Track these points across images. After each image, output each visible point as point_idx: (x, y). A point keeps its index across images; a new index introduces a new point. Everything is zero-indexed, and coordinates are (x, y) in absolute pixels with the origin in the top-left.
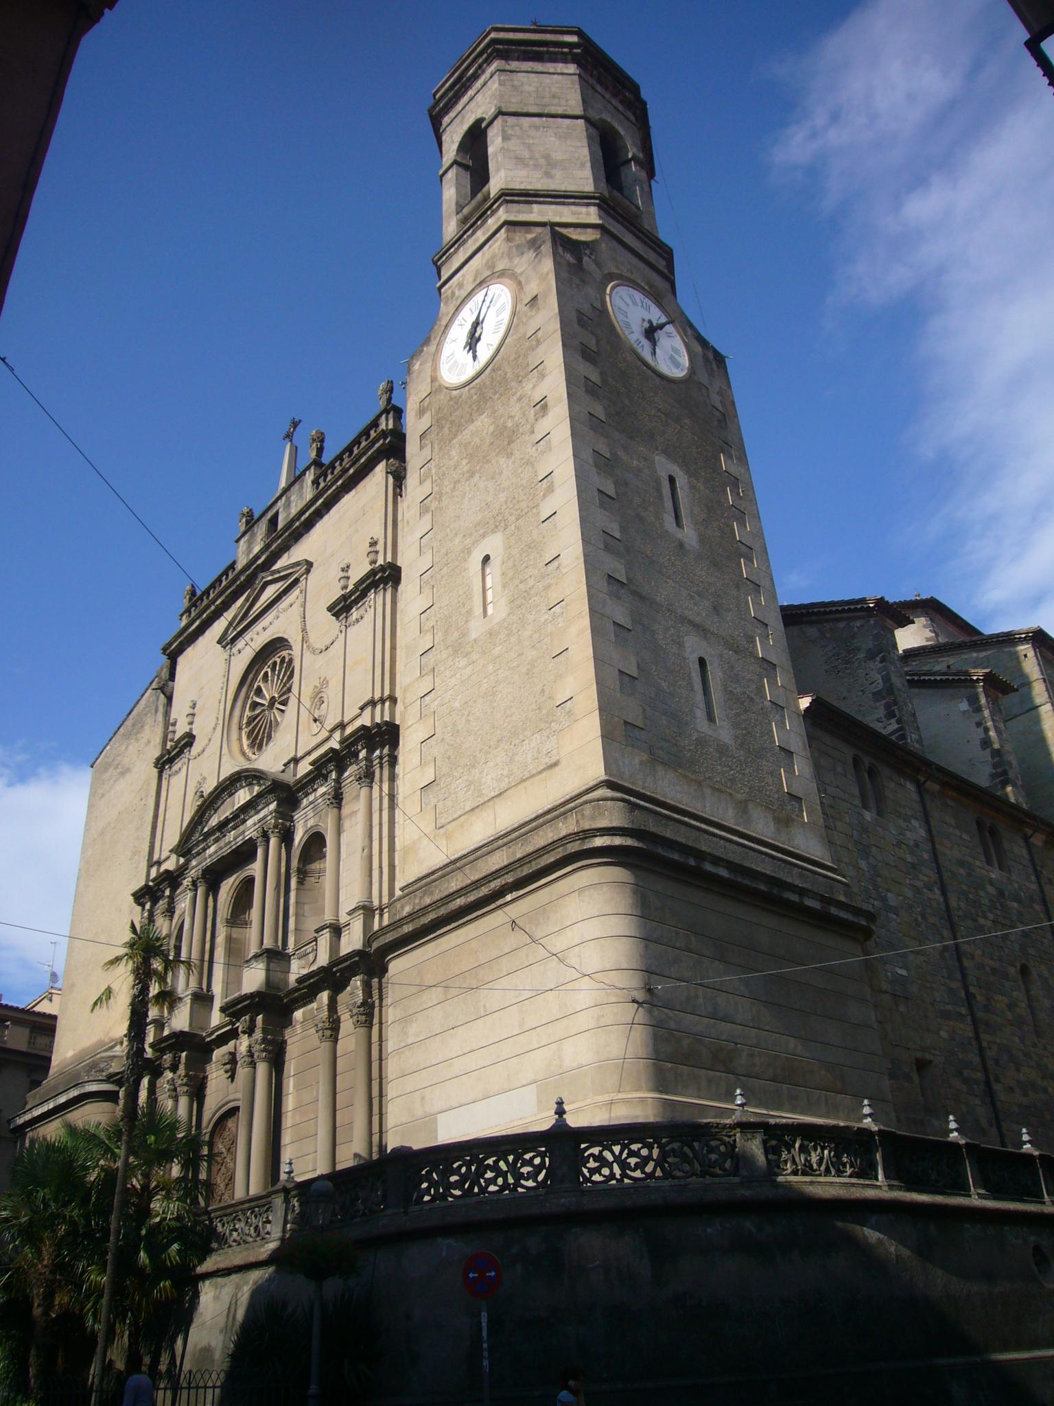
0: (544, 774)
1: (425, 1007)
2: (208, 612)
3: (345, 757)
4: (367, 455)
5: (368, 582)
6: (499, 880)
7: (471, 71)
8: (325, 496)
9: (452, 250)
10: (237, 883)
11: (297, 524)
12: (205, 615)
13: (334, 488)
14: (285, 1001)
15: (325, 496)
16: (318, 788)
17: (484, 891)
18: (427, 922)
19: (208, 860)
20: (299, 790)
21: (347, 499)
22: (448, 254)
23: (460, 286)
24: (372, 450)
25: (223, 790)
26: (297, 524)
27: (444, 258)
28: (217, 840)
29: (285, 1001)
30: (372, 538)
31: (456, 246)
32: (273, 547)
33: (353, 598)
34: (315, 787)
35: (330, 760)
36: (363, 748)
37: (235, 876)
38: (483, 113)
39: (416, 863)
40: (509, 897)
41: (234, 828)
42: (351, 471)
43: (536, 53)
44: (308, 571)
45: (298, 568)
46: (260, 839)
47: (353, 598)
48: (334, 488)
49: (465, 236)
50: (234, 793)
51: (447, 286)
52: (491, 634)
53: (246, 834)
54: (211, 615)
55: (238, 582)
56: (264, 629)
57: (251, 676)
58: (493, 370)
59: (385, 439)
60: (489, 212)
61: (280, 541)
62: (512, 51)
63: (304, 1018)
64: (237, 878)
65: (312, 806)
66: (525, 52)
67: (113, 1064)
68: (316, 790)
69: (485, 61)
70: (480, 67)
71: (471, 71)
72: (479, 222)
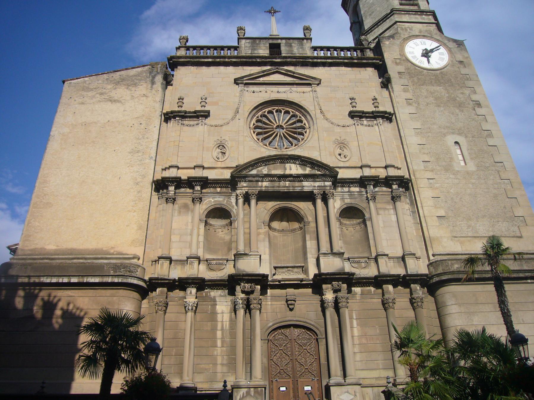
0: (515, 239)
1: (482, 311)
2: (222, 60)
3: (380, 183)
4: (368, 61)
5: (381, 114)
6: (530, 274)
8: (334, 60)
10: (277, 207)
11: (310, 60)
12: (218, 60)
13: (341, 61)
14: (354, 281)
15: (334, 60)
16: (352, 187)
17: (521, 275)
18: (487, 277)
19: (264, 188)
20: (339, 183)
21: (343, 68)
22: (400, 12)
23: (411, 29)
24: (372, 61)
25: (278, 159)
26: (310, 60)
27: (398, 12)
28: (271, 181)
29: (354, 281)
30: (375, 96)
31: (405, 12)
32: (289, 60)
33: (367, 115)
34: (351, 186)
35: (373, 180)
36: (396, 184)
37: (279, 203)
39: (440, 246)
40: (529, 281)
41: (290, 181)
42: (356, 61)
44: (318, 85)
45: (313, 80)
46: (320, 195)
47: (367, 115)
48: (341, 61)
49: (411, 13)
50: (285, 163)
52: (468, 173)
53: (305, 188)
54: (222, 62)
55: (254, 60)
56: (278, 92)
57: (261, 107)
58: (441, 73)
59: (380, 62)
60: (425, 13)
61: (294, 60)
63: (361, 293)
64: (279, 204)
65: (349, 193)
67: (139, 270)
68: (350, 187)
72: (419, 13)
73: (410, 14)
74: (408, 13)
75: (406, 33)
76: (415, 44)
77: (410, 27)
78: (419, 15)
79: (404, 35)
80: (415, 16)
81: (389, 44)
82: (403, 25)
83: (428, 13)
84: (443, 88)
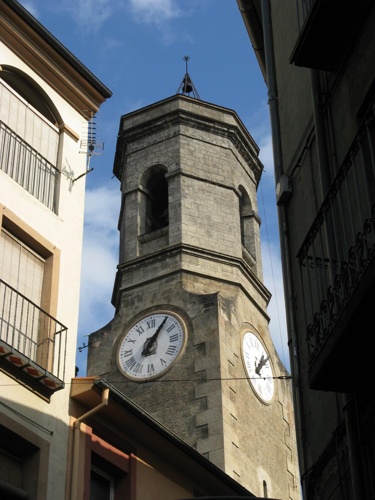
7: (159, 123)
9: (135, 266)
22: (130, 267)
31: (138, 265)
38: (166, 163)
43: (206, 126)
51: (127, 293)
60: (169, 254)
62: (191, 121)
66: (199, 123)
69: (171, 121)
70: (166, 123)
71: (159, 123)
72: (159, 257)
73: (146, 265)
74: (143, 263)
75: (131, 311)
76: (138, 331)
77: (140, 294)
78: (160, 261)
79: (127, 316)
80: (154, 266)
81: (101, 345)
82: (130, 295)
83: (174, 252)
84: (158, 415)
